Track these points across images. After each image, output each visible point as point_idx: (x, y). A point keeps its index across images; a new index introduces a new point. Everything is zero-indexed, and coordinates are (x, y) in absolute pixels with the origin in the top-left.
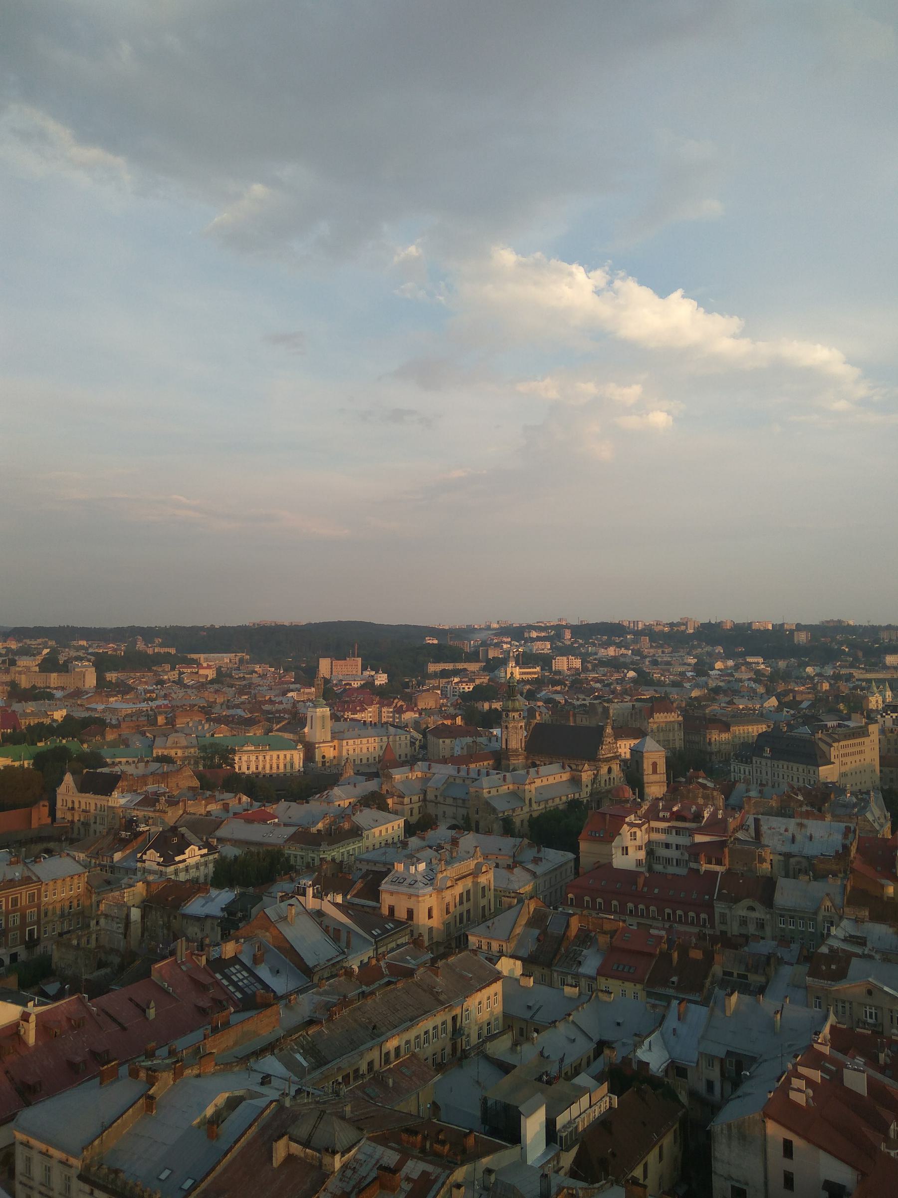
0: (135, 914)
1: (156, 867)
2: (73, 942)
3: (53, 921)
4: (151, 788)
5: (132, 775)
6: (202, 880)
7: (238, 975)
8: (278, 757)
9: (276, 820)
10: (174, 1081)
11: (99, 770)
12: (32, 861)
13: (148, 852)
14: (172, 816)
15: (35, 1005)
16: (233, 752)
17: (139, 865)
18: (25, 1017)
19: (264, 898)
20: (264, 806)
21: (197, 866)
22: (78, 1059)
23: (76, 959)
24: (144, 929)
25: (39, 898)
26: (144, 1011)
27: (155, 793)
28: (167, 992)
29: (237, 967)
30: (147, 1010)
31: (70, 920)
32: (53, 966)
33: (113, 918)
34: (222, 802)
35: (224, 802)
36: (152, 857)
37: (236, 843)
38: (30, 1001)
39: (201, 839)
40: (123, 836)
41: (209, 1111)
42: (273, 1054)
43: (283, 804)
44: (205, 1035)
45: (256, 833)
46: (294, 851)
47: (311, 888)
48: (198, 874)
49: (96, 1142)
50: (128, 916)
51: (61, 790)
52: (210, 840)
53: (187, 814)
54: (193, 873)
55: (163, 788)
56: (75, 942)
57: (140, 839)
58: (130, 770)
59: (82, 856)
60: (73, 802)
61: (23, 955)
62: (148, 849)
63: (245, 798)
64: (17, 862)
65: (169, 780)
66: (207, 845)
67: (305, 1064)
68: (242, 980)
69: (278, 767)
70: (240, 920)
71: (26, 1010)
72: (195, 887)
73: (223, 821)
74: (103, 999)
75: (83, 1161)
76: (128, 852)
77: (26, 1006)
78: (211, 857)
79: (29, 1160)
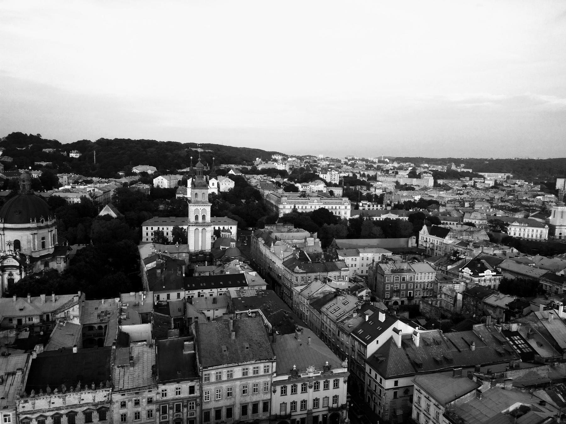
0: (460, 297)
1: (469, 277)
2: (429, 302)
3: (419, 291)
4: (465, 237)
5: (455, 230)
6: (492, 287)
7: (519, 341)
8: (537, 231)
9: (534, 264)
10: (491, 387)
11: (439, 226)
12: (410, 262)
13: (465, 269)
14: (477, 252)
15: (419, 329)
16: (508, 225)
17: (460, 273)
18: (415, 333)
19: (531, 305)
20: (526, 256)
21: (490, 280)
22: (438, 359)
23: (431, 310)
24: (463, 304)
25: (414, 279)
26: (470, 346)
27: (467, 241)
28: (481, 340)
29: (518, 337)
30: (471, 346)
31: (427, 292)
32: (420, 311)
33: (448, 296)
34: (502, 250)
35: (504, 250)
36: (467, 271)
37: (511, 272)
38: (417, 327)
39: (493, 267)
40: (452, 258)
41: (511, 408)
42: (544, 390)
43: (538, 257)
44: (506, 369)
45: (522, 269)
46: (546, 284)
47: (563, 307)
48: (490, 284)
49: (452, 403)
50: (456, 297)
51: (421, 232)
52: (498, 268)
53: (484, 253)
54: (488, 283)
55: (470, 238)
56: (430, 302)
57: (460, 262)
58: (454, 227)
59: (432, 264)
60: (427, 238)
61: (406, 302)
62: (465, 267)
63: (515, 250)
64: (405, 262)
65: (474, 235)
66: (495, 270)
67: (563, 400)
68: (520, 344)
69: (532, 236)
70: (517, 313)
71: (415, 330)
72: (489, 290)
73: (503, 260)
74: (449, 335)
75: (446, 409)
76: (454, 266)
77: (415, 328)
78: (498, 277)
79: (419, 398)
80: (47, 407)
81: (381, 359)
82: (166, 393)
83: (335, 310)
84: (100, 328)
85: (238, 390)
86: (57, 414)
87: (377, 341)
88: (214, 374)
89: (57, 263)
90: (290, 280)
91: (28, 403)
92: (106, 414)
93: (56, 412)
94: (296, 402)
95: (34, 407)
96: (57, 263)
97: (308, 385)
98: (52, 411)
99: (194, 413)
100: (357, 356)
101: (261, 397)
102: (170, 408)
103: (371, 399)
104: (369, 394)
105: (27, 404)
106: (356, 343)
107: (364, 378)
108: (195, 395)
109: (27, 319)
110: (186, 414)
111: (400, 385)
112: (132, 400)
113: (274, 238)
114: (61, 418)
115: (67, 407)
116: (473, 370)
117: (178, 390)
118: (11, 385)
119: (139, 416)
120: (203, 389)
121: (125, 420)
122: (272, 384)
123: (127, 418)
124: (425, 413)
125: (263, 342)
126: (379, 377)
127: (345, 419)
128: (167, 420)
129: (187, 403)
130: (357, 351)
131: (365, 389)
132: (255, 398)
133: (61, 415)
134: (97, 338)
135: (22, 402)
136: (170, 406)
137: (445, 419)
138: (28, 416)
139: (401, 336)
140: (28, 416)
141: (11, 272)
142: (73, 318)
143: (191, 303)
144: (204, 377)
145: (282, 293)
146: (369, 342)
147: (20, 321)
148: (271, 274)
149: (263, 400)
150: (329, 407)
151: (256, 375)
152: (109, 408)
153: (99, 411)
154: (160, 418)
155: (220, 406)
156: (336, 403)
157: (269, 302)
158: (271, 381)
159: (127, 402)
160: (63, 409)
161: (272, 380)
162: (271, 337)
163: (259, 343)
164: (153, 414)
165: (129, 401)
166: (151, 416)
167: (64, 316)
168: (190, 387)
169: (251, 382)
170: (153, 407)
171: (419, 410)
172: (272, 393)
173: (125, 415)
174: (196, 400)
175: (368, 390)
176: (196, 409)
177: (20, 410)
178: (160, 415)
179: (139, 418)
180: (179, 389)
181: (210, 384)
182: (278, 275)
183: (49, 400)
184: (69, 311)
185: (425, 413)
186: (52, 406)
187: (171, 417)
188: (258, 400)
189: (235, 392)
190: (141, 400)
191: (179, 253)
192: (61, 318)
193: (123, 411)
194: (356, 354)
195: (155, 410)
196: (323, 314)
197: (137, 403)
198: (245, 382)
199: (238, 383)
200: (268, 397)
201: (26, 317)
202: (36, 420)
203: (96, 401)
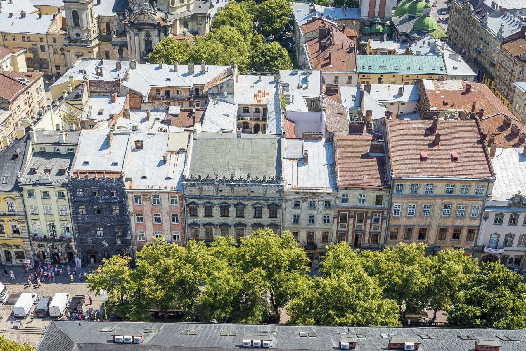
80: (215, 194)
82: (347, 199)
84: (257, 111)
85: (438, 209)
86: (225, 203)
88: (409, 185)
89: (198, 24)
90: (511, 72)
91: (195, 186)
92: (276, 211)
93: (224, 201)
94: (514, 236)
95: (201, 193)
96: (198, 24)
98: (220, 199)
99: (378, 227)
101: (467, 222)
102: (351, 217)
105: (194, 188)
108: (383, 206)
109: (176, 92)
110: (369, 227)
112: (307, 201)
113: (490, 5)
114: (229, 209)
115: (236, 198)
117: (362, 198)
118: (176, 165)
119: (313, 220)
120: (393, 201)
121: (298, 221)
122: (483, 209)
123: (300, 221)
128: (346, 229)
129: (372, 215)
132: (458, 223)
133: (229, 206)
134: (253, 123)
135: (189, 185)
136: (351, 214)
138: (195, 200)
140: (195, 200)
141: (148, 32)
142: (227, 96)
143: (369, 91)
144: (396, 187)
145: (494, 89)
147: (168, 93)
148: (479, 58)
149: (468, 226)
151: (464, 195)
152: (281, 206)
153: (269, 206)
154: (337, 226)
155: (412, 224)
157: (481, 101)
159: (301, 202)
160: (231, 199)
161: (484, 203)
162: (489, 149)
163: (472, 155)
164: (330, 221)
165: (304, 201)
166: (328, 222)
167: (217, 92)
168: (377, 197)
169: (455, 202)
170: (331, 213)
173: (298, 216)
174: (383, 213)
176: (382, 222)
177: (187, 193)
178: (338, 223)
179: (313, 222)
180: (364, 196)
181: (403, 197)
182: (491, 63)
183: (216, 187)
184: (223, 86)
186: (220, 194)
187: (351, 227)
188: (462, 224)
189: (433, 211)
190: (317, 203)
191: (346, 19)
192: (213, 94)
193: (296, 211)
195: (332, 216)
197: (313, 205)
198: (448, 201)
199: (439, 201)
200: (476, 223)
201: (174, 88)
202: (203, 206)
203: (267, 196)
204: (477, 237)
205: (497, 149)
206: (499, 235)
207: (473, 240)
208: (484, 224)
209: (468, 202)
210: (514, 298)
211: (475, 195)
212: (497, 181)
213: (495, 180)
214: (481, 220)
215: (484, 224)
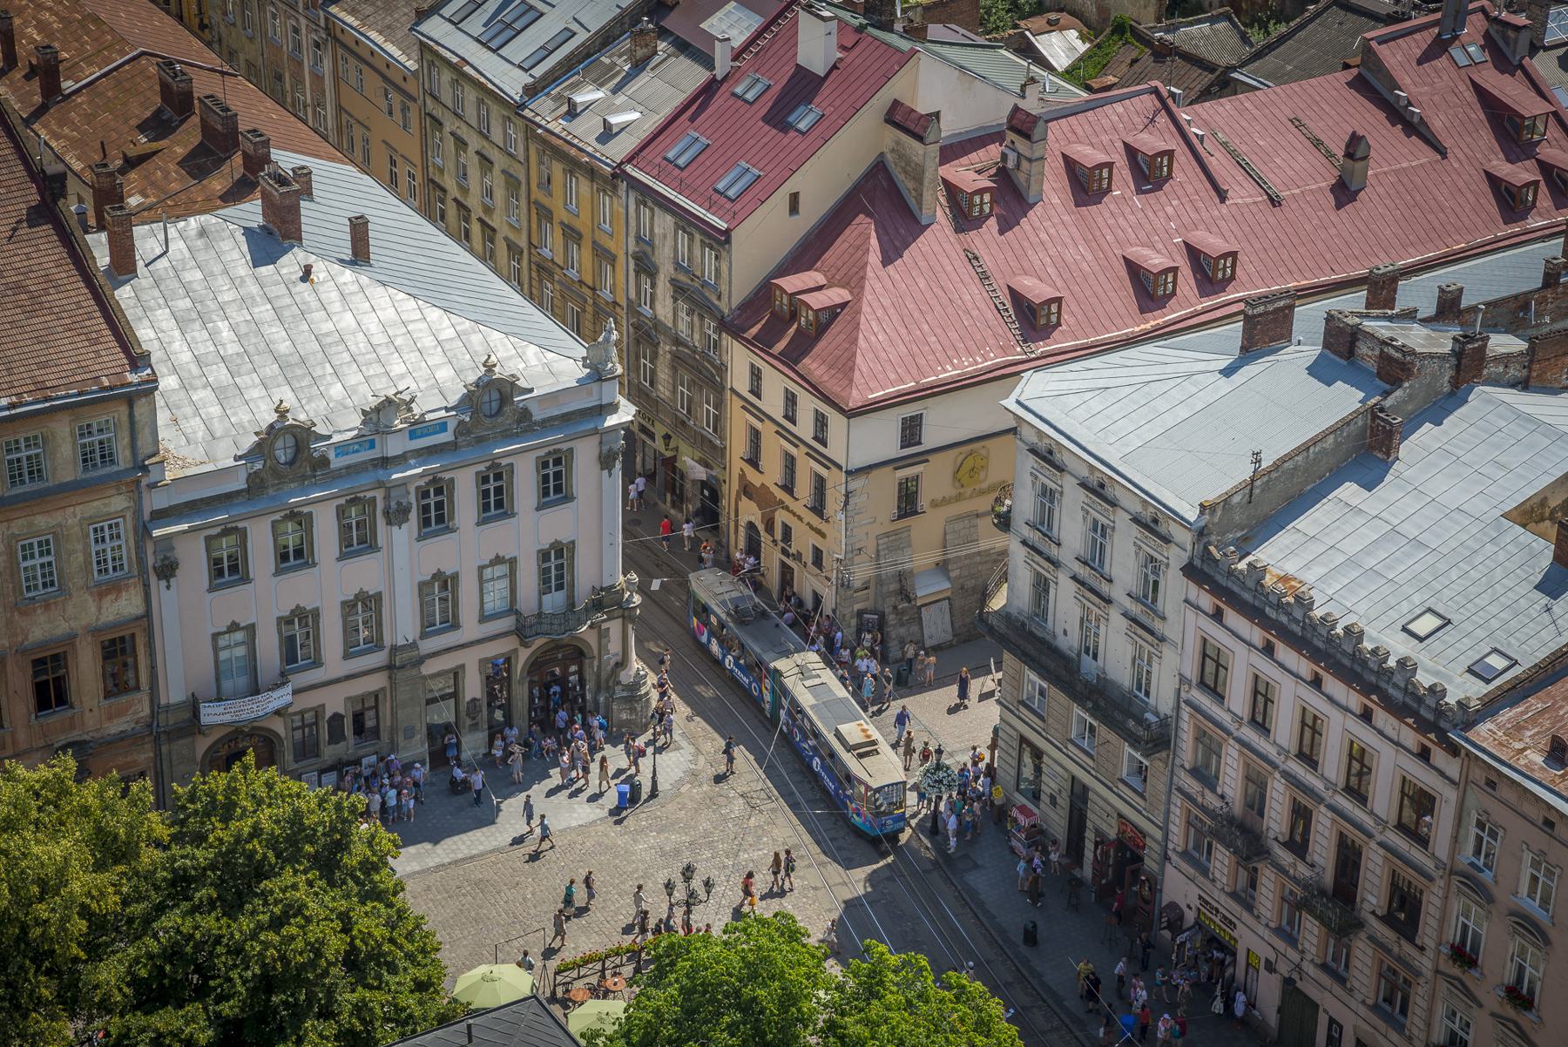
22: (1155, 261)
81: (817, 301)
83: (509, 26)
87: (794, 198)
94: (316, 613)
97: (380, 506)
100: (669, 301)
103: (765, 537)
104: (750, 512)
106: (664, 223)
107: (718, 423)
111: (932, 436)
116: (1351, 303)
122: (143, 532)
124: (1083, 572)
125: (47, 278)
126: (808, 405)
127: (622, 664)
130: (666, 271)
131: (731, 488)
137: (1194, 591)
139: (936, 147)
146: (740, 205)
149: (95, 631)
150: (517, 613)
151: (28, 487)
156: (560, 587)
158: (138, 511)
161: (138, 502)
171: (1048, 559)
172: (153, 579)
175: (747, 490)
185: (1083, 572)
188: (62, 628)
194: (664, 289)
196: (428, 56)
200: (128, 604)
204: (153, 668)
205: (138, 231)
206: (251, 629)
207: (137, 688)
208: (167, 599)
209: (58, 517)
210: (343, 905)
211: (80, 475)
212: (168, 382)
213: (153, 380)
214: (146, 586)
215: (167, 599)
